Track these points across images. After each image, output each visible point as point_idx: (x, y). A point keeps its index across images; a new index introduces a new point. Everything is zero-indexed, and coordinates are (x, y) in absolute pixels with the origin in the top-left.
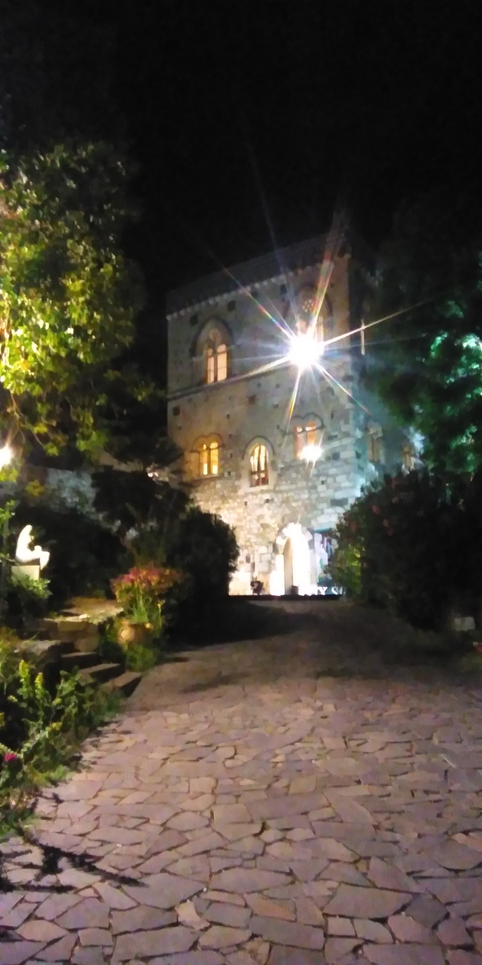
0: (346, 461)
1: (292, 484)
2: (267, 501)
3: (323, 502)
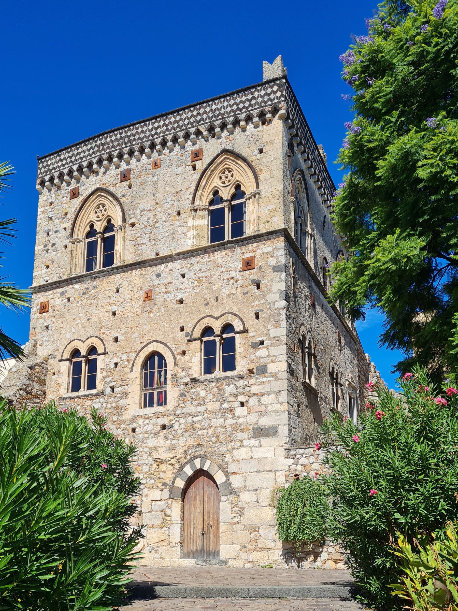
1: (199, 405)
3: (241, 431)
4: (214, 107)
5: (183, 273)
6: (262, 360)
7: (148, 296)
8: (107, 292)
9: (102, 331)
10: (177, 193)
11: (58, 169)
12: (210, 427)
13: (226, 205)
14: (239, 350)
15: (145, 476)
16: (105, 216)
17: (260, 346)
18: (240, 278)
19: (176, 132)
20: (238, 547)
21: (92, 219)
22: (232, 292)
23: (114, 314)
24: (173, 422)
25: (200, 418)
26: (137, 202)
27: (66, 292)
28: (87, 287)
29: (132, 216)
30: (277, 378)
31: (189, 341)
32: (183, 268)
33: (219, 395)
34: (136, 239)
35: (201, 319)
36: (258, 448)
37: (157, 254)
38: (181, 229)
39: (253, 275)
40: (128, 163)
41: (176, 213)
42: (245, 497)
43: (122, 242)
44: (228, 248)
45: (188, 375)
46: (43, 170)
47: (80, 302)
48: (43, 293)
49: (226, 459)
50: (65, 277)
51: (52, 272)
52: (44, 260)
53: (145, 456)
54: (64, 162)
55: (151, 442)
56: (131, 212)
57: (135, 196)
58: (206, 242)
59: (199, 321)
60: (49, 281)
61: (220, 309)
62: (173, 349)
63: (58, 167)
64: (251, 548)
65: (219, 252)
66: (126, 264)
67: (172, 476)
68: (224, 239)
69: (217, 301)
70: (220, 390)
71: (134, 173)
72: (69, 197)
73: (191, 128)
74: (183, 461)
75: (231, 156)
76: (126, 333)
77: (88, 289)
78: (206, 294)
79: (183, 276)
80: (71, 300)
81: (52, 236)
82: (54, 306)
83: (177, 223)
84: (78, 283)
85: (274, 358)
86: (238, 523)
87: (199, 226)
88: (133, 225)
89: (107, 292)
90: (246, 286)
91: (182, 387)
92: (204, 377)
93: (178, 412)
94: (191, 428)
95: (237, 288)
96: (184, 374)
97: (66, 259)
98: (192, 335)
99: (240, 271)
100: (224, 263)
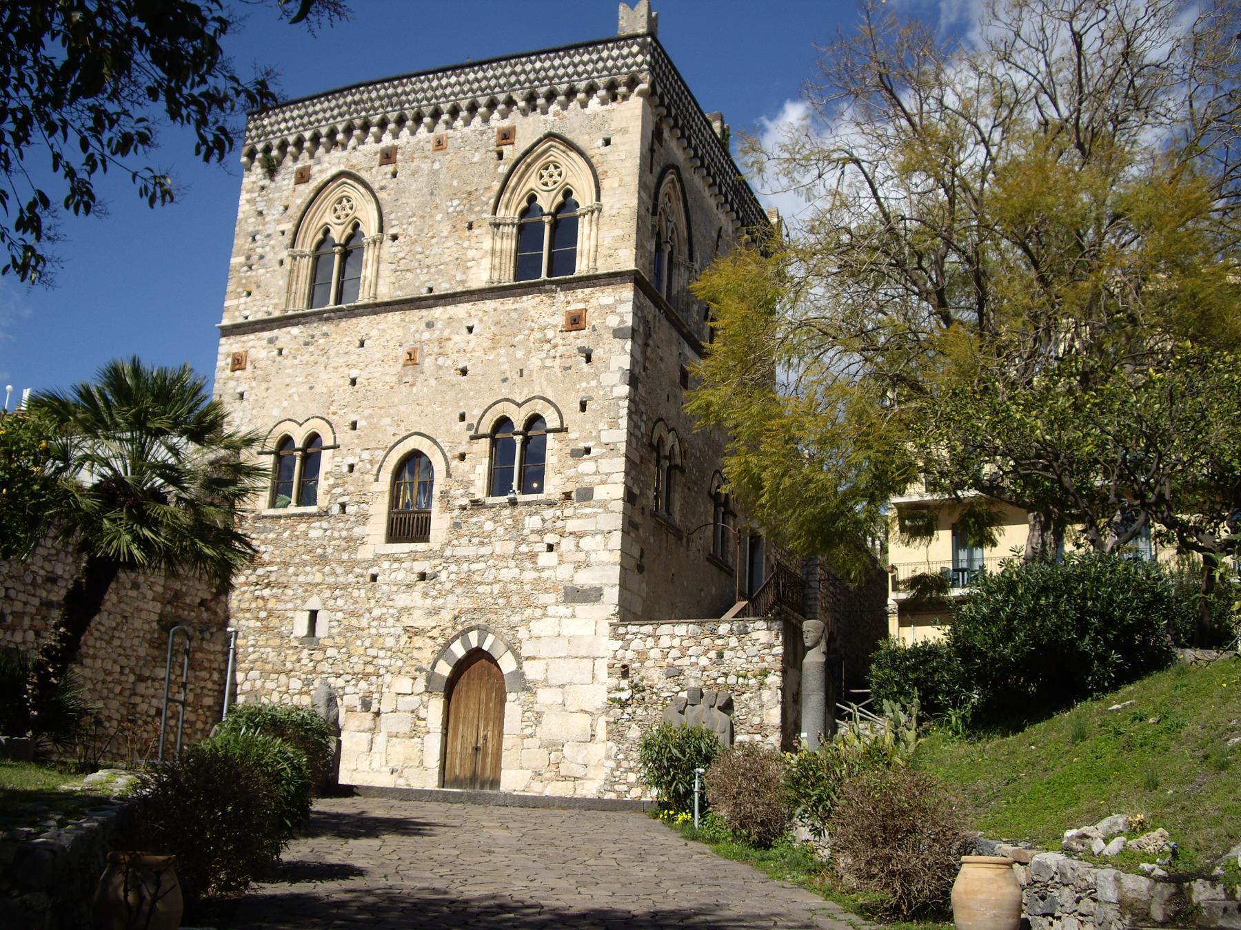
0: (604, 505)
1: (482, 544)
2: (423, 577)
3: (546, 591)
6: (587, 479)
7: (411, 358)
9: (333, 409)
10: (470, 193)
12: (496, 581)
14: (551, 460)
15: (389, 653)
16: (350, 218)
17: (586, 456)
20: (529, 773)
23: (353, 382)
24: (439, 569)
25: (481, 565)
26: (404, 200)
29: (394, 223)
30: (607, 511)
31: (472, 438)
33: (514, 532)
35: (495, 404)
36: (571, 620)
37: (431, 290)
39: (582, 339)
40: (396, 136)
42: (545, 696)
44: (545, 291)
45: (467, 494)
46: (254, 133)
48: (238, 338)
49: (519, 635)
53: (390, 622)
54: (290, 124)
55: (402, 600)
56: (392, 217)
57: (401, 191)
58: (508, 278)
59: (490, 407)
60: (251, 319)
61: (526, 391)
62: (446, 450)
64: (548, 775)
66: (378, 301)
67: (431, 657)
70: (516, 521)
74: (450, 633)
76: (371, 416)
77: (313, 337)
79: (470, 330)
80: (284, 352)
81: (259, 243)
84: (297, 324)
85: (604, 477)
86: (531, 736)
88: (395, 238)
90: (570, 357)
91: (457, 512)
92: (491, 500)
93: (448, 553)
94: (466, 582)
96: (461, 491)
97: (281, 283)
98: (477, 429)
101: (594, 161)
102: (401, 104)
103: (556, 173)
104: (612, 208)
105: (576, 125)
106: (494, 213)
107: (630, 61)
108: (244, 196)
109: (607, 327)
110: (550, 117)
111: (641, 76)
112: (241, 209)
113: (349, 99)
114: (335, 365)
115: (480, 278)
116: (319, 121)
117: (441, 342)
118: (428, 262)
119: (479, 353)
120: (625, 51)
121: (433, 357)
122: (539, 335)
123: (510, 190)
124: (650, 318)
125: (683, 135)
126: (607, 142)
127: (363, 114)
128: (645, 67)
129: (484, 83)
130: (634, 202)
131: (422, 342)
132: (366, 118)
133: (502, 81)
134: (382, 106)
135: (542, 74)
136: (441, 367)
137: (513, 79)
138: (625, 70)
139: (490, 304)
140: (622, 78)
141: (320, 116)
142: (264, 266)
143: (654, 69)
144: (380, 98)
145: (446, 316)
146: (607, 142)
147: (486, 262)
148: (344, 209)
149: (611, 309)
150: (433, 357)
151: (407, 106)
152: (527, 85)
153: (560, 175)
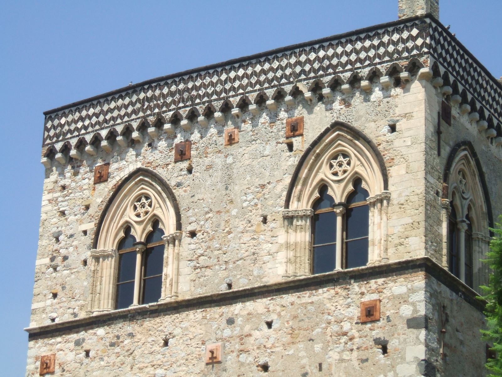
4: (322, 54)
5: (269, 320)
8: (149, 345)
10: (263, 186)
11: (76, 133)
13: (338, 211)
16: (149, 216)
18: (357, 334)
19: (262, 89)
21: (128, 219)
22: (345, 357)
26: (200, 197)
27: (84, 340)
28: (117, 334)
32: (269, 311)
34: (197, 258)
37: (230, 286)
38: (267, 247)
39: (378, 331)
41: (261, 219)
43: (176, 262)
47: (106, 358)
48: (46, 340)
50: (82, 315)
51: (62, 305)
52: (50, 283)
54: (87, 122)
56: (190, 213)
58: (304, 272)
60: (57, 321)
63: (77, 129)
65: (325, 289)
68: (333, 267)
69: (320, 369)
71: (197, 149)
72: (92, 182)
73: (287, 84)
75: (347, 133)
77: (118, 337)
78: (303, 357)
79: (269, 325)
81: (63, 244)
82: (63, 363)
83: (262, 237)
87: (296, 244)
88: (193, 234)
89: (149, 345)
90: (367, 348)
95: (352, 350)
97: (85, 283)
99: (357, 323)
100: (333, 308)
101: (380, 148)
102: (192, 98)
103: (345, 161)
104: (400, 195)
105: (362, 113)
106: (287, 205)
107: (410, 44)
108: (46, 197)
109: (401, 317)
110: (337, 105)
111: (422, 60)
112: (43, 209)
113: (142, 95)
114: (141, 365)
115: (277, 271)
116: (113, 119)
117: (242, 338)
118: (225, 258)
119: (279, 349)
120: (405, 35)
121: (235, 354)
122: (335, 328)
123: (301, 182)
124: (447, 303)
125: (474, 109)
126: (393, 128)
127: (157, 110)
128: (425, 50)
129: (271, 75)
130: (420, 187)
131: (222, 339)
132: (158, 114)
133: (288, 71)
134: (174, 102)
135: (326, 62)
136: (242, 364)
137: (298, 69)
138: (405, 54)
139: (288, 298)
140: (404, 63)
141: (116, 113)
142: (67, 267)
143: (435, 50)
144: (172, 94)
145: (245, 313)
146: (393, 128)
147: (282, 256)
148: (143, 206)
149: (403, 299)
150: (235, 354)
151: (198, 101)
152: (312, 75)
153: (349, 164)
